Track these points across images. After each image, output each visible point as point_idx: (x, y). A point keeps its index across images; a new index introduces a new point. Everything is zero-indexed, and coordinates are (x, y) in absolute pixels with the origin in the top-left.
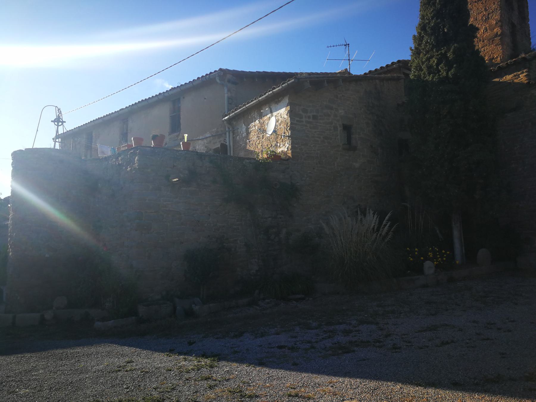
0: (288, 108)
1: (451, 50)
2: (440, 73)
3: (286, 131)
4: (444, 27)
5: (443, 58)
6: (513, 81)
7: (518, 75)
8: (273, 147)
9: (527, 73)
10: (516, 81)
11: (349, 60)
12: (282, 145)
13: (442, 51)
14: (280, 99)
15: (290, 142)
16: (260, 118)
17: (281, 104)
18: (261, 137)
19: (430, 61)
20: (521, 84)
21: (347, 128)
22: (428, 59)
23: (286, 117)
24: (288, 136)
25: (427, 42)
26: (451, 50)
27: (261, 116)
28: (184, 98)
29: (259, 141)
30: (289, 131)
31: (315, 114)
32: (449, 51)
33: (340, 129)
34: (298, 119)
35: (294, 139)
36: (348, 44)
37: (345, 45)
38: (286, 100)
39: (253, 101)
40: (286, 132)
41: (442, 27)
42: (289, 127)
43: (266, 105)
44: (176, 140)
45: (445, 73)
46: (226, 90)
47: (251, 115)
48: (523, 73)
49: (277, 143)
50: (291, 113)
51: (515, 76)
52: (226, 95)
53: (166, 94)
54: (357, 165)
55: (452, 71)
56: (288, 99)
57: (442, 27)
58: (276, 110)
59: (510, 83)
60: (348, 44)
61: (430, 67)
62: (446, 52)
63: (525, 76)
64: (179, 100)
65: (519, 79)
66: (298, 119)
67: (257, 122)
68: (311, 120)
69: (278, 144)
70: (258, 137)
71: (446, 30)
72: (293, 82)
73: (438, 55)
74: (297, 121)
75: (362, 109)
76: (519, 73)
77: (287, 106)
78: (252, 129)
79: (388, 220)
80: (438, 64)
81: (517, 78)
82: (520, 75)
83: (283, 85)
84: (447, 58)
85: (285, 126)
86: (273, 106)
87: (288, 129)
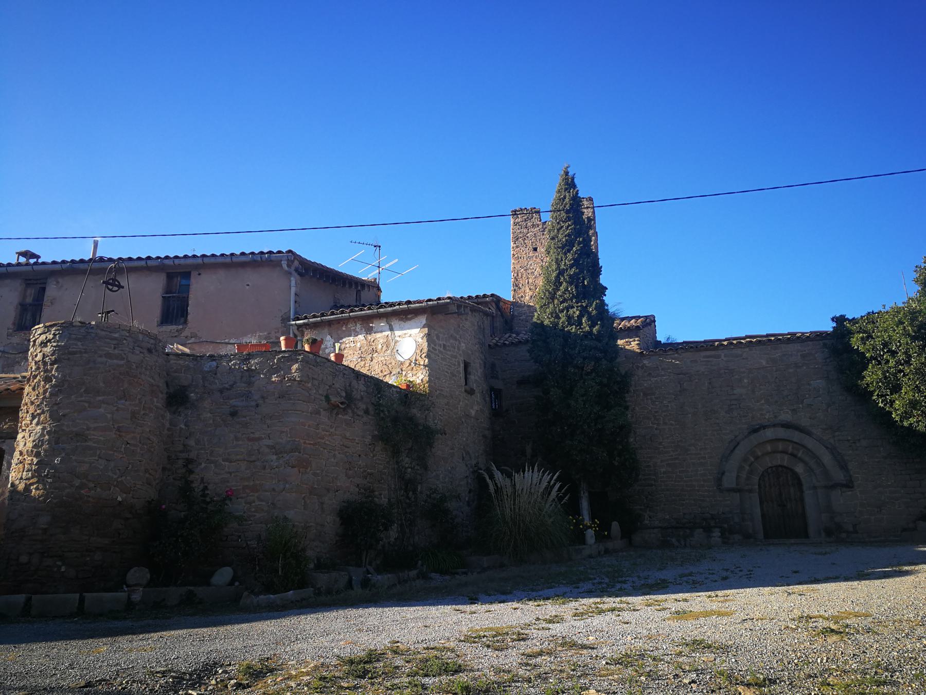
0: (426, 330)
1: (594, 306)
2: (582, 327)
3: (418, 357)
4: (584, 279)
5: (584, 311)
6: (624, 347)
7: (630, 342)
8: (394, 375)
9: (638, 342)
10: (627, 347)
11: (379, 267)
12: (411, 375)
13: (583, 304)
14: (409, 316)
15: (426, 372)
16: (367, 334)
17: (412, 322)
18: (369, 358)
19: (568, 311)
20: (633, 352)
21: (466, 365)
22: (568, 308)
23: (420, 340)
24: (424, 365)
25: (566, 290)
26: (594, 306)
27: (369, 331)
28: (199, 274)
29: (364, 363)
30: (425, 359)
31: (445, 343)
32: (591, 305)
33: (462, 365)
34: (433, 346)
35: (432, 368)
36: (380, 247)
37: (375, 246)
38: (423, 320)
39: (364, 310)
40: (420, 359)
41: (581, 278)
42: (425, 355)
43: (380, 319)
44: (176, 336)
45: (587, 328)
46: (293, 283)
47: (346, 325)
48: (634, 341)
49: (402, 371)
50: (429, 336)
51: (627, 342)
52: (293, 290)
53: (167, 262)
54: (473, 413)
55: (597, 327)
56: (425, 319)
57: (581, 278)
58: (402, 329)
59: (621, 348)
60: (380, 247)
61: (569, 318)
62: (586, 307)
63: (637, 344)
64: (187, 275)
65: (631, 346)
66: (433, 346)
67: (361, 337)
68: (442, 349)
69: (404, 373)
70: (361, 357)
71: (586, 283)
72: (447, 303)
73: (577, 307)
74: (433, 348)
75: (477, 346)
76: (631, 340)
77: (424, 327)
78: (348, 345)
79: (556, 481)
80: (580, 317)
81: (629, 345)
82: (632, 343)
83: (428, 303)
84: (589, 313)
85: (418, 351)
86: (395, 323)
87: (423, 356)
